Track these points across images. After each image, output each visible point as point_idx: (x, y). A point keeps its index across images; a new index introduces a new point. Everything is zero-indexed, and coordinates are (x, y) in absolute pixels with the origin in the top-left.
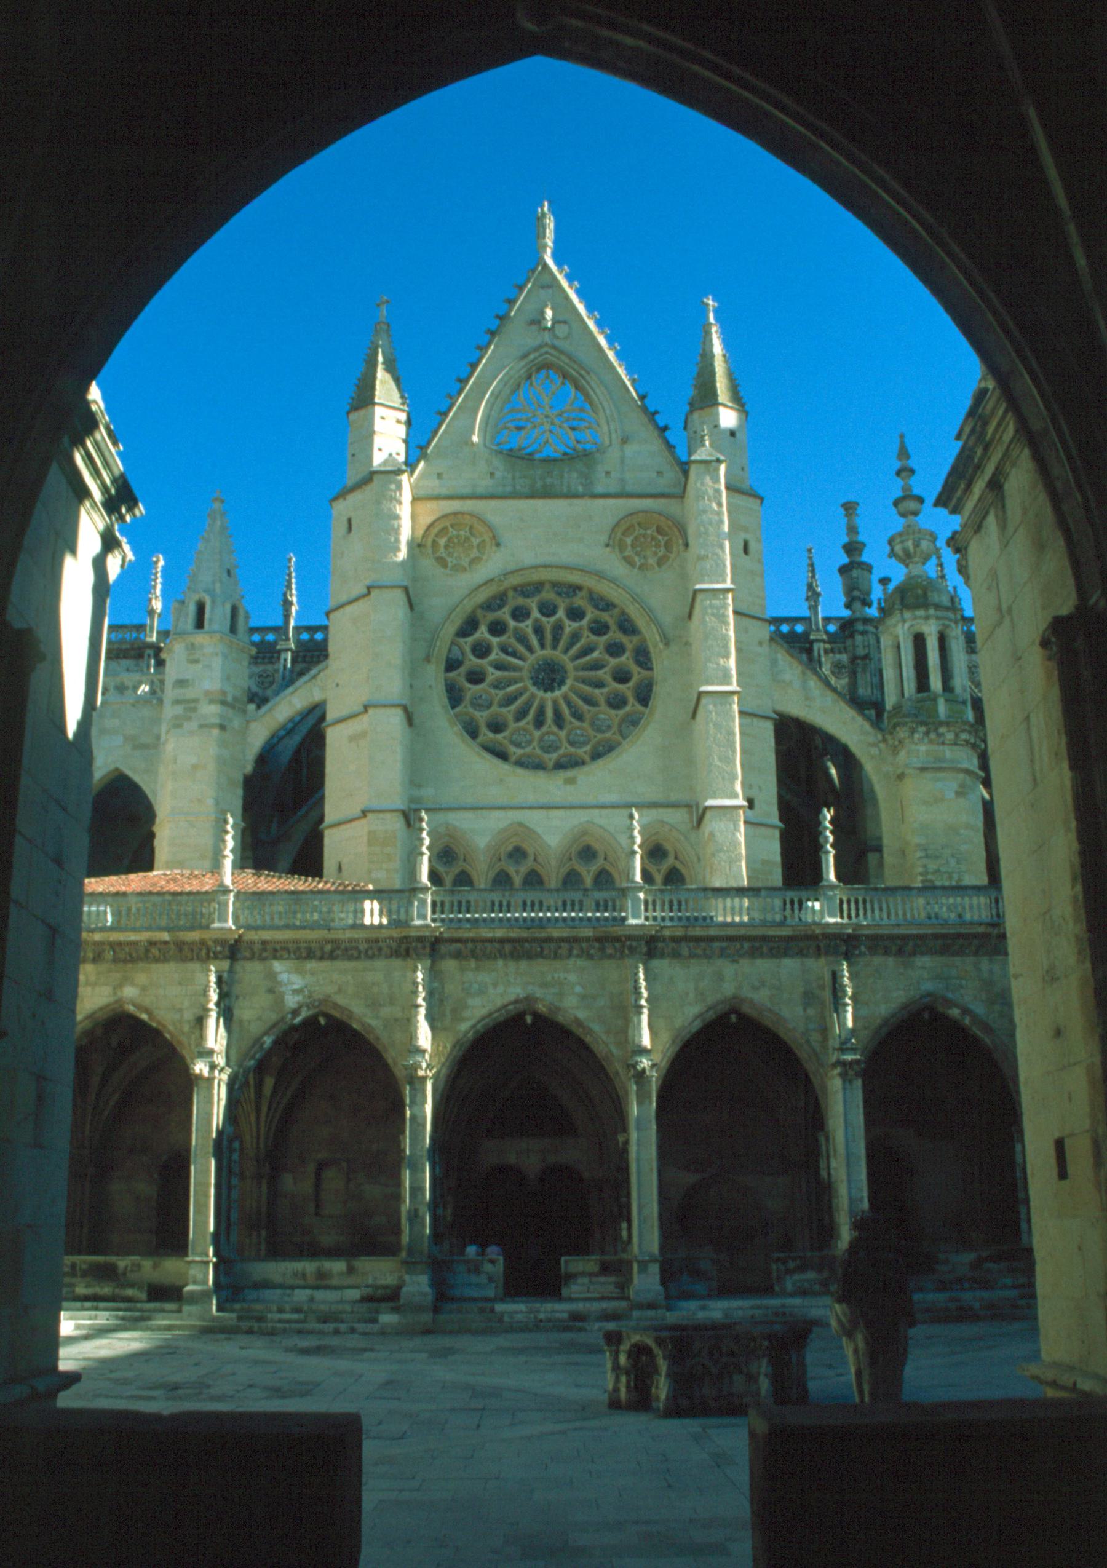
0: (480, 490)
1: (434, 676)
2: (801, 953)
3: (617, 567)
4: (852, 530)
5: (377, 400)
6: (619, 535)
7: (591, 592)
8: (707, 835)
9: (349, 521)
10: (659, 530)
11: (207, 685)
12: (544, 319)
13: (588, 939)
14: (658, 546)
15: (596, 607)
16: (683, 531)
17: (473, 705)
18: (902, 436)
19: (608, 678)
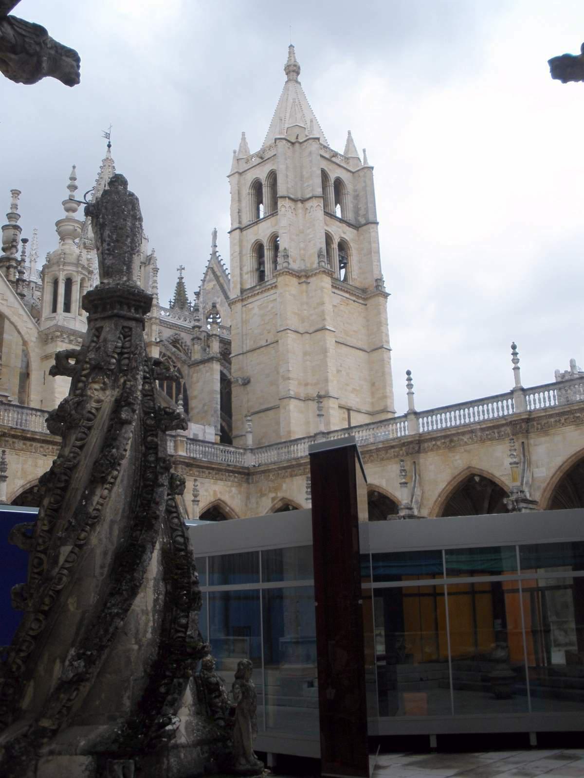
4: (14, 206)
18: (74, 167)
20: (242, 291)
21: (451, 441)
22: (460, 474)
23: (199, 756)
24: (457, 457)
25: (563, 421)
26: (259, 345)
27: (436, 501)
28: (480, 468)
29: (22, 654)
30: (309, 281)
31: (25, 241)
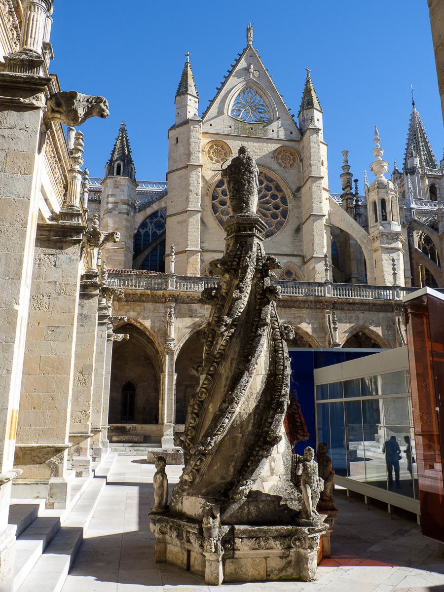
0: (226, 133)
1: (208, 200)
2: (386, 311)
3: (275, 166)
5: (189, 92)
6: (276, 154)
7: (265, 174)
8: (311, 267)
9: (177, 138)
10: (291, 153)
11: (122, 197)
12: (250, 68)
13: (311, 301)
14: (290, 160)
15: (267, 180)
16: (300, 154)
17: (222, 214)
19: (272, 208)
23: (275, 508)
29: (189, 437)
31: (356, 181)
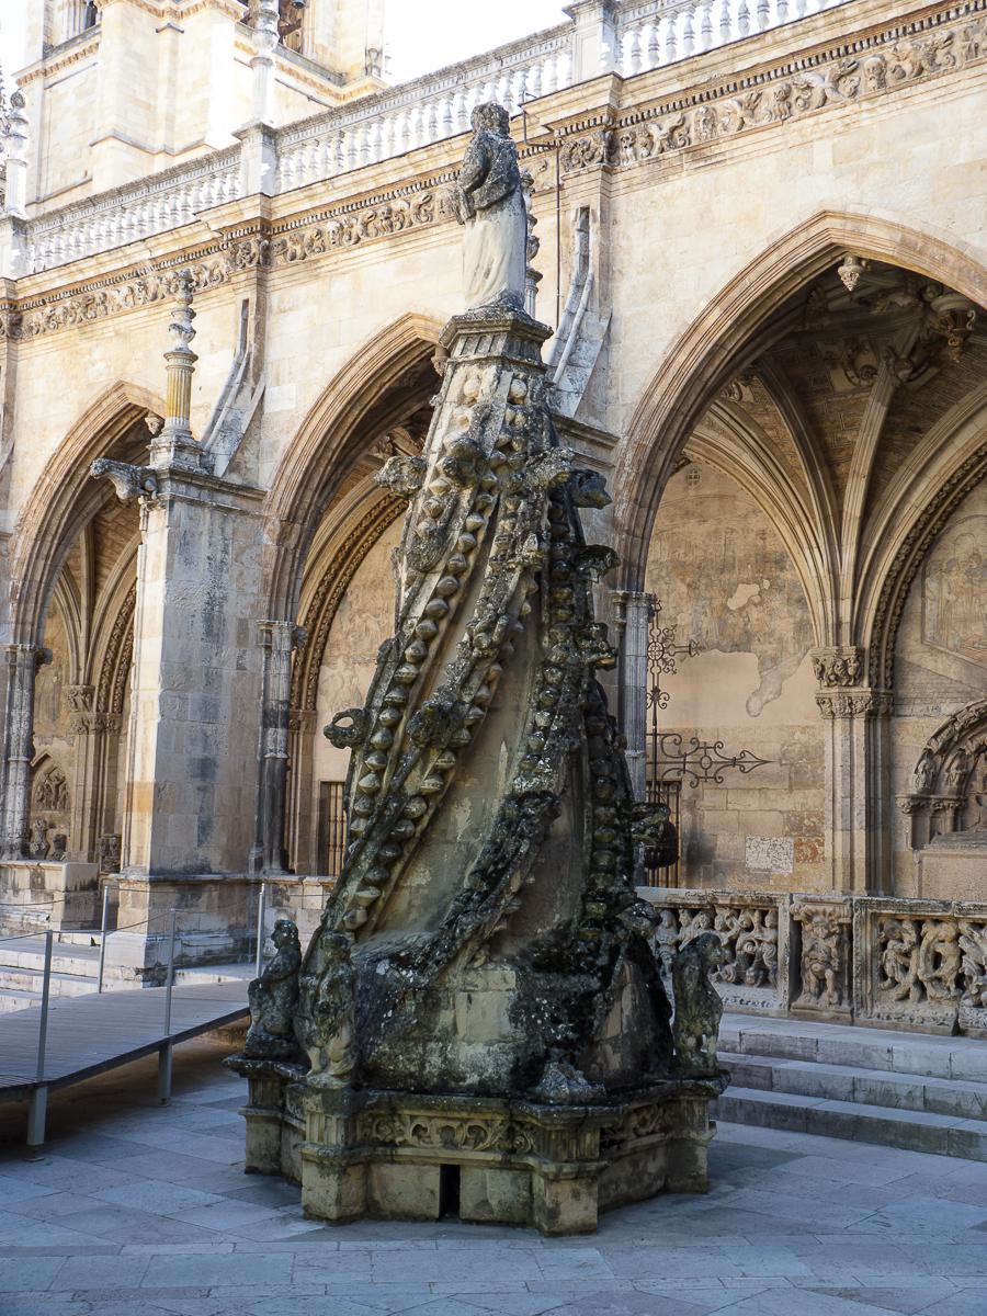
20: (49, 50)
21: (88, 304)
22: (98, 404)
24: (97, 354)
25: (357, 229)
26: (70, 183)
27: (37, 488)
28: (144, 386)
30: (182, 25)
